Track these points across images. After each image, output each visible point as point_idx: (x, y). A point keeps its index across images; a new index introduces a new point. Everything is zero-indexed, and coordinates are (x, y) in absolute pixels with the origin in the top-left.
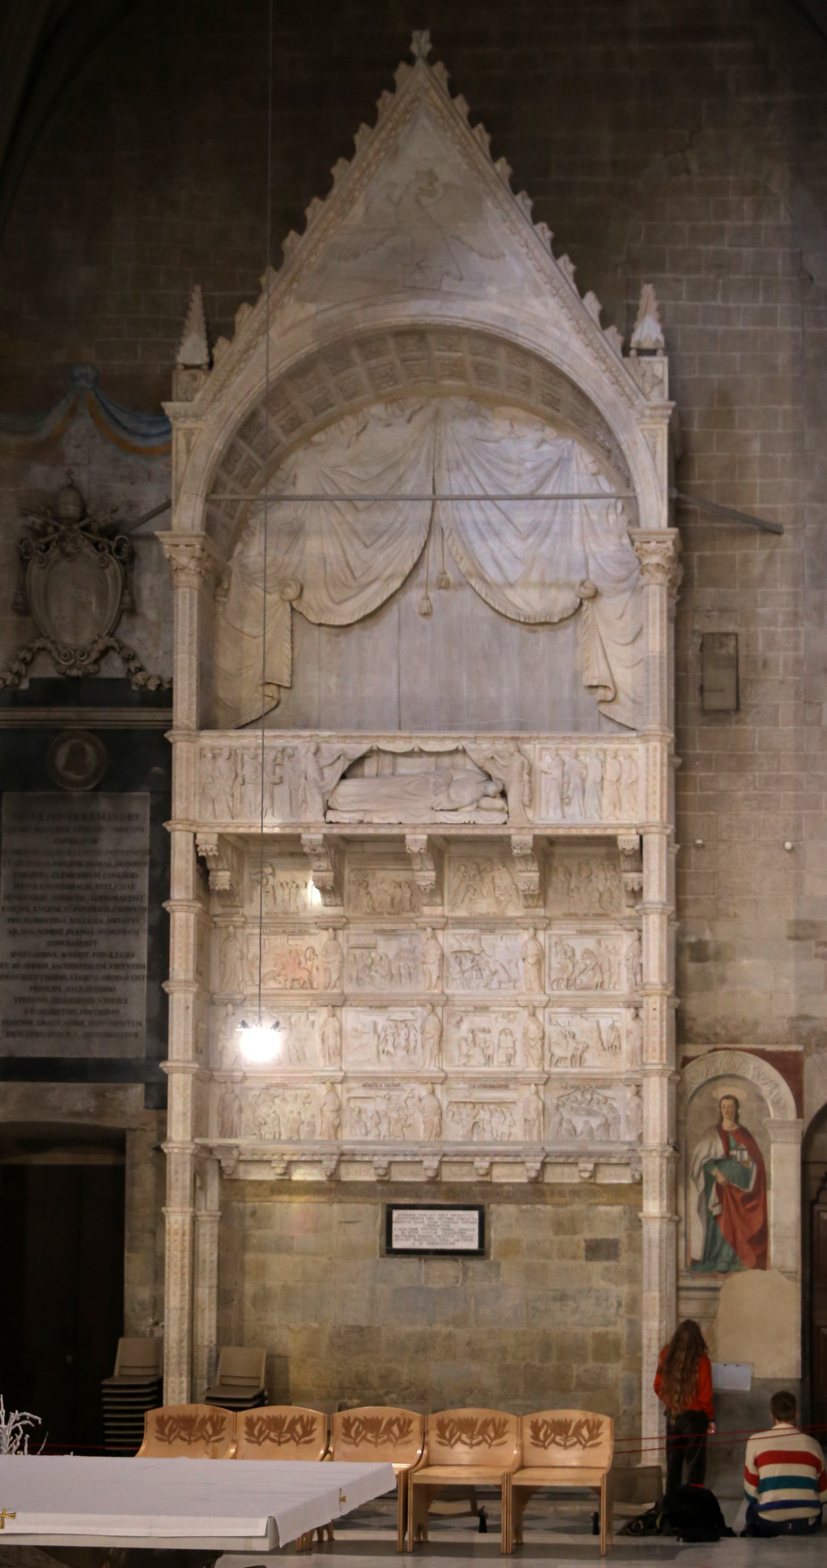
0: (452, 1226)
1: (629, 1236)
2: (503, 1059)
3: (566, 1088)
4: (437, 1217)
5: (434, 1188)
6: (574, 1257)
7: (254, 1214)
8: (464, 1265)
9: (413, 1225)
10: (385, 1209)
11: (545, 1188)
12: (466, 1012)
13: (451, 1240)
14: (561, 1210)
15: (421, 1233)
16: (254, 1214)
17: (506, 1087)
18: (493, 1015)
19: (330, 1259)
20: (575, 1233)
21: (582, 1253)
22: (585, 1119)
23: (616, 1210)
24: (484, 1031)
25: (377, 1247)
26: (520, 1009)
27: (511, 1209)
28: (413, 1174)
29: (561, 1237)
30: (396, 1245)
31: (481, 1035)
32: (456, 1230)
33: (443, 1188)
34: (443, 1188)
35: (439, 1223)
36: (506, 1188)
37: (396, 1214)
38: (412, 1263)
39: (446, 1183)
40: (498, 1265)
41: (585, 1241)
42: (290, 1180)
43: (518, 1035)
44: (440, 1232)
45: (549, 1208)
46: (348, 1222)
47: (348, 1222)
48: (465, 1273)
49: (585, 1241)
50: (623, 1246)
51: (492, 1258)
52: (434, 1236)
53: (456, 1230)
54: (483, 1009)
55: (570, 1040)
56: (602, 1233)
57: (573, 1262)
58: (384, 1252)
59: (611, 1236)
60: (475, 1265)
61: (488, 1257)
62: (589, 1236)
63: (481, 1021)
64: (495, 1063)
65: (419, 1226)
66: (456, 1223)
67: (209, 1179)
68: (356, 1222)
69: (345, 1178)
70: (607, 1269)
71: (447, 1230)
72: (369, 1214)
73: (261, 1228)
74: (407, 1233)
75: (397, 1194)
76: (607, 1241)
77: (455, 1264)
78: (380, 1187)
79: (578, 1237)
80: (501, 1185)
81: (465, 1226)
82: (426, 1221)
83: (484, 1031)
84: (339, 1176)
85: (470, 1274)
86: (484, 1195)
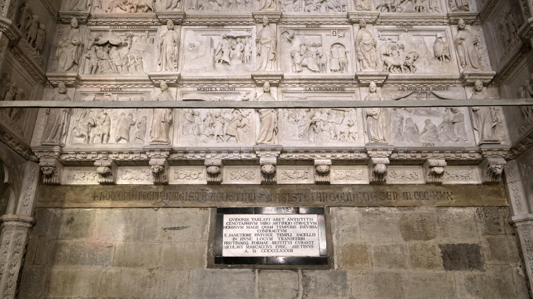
0: (289, 231)
1: (489, 240)
2: (336, 67)
3: (403, 90)
4: (272, 222)
5: (268, 191)
6: (431, 266)
7: (70, 221)
8: (304, 276)
9: (245, 231)
10: (215, 213)
11: (388, 190)
12: (298, 30)
13: (289, 246)
14: (408, 212)
15: (254, 239)
16: (70, 221)
17: (342, 90)
18: (323, 34)
19: (151, 270)
20: (428, 238)
21: (439, 260)
22: (426, 118)
23: (469, 212)
24: (314, 46)
25: (205, 256)
26: (350, 26)
27: (354, 211)
28: (245, 177)
29: (413, 242)
30: (226, 253)
31: (313, 49)
32: (294, 235)
33: (278, 190)
34: (278, 190)
35: (275, 227)
36: (346, 190)
37: (227, 218)
38: (243, 275)
39: (281, 185)
40: (344, 274)
41: (440, 246)
42: (113, 184)
43: (350, 46)
44: (275, 238)
45: (394, 210)
46: (174, 229)
47: (174, 229)
48: (306, 286)
49: (440, 246)
50: (485, 253)
51: (336, 267)
52: (270, 242)
53: (294, 235)
54: (313, 26)
55: (401, 51)
56: (457, 237)
57: (430, 271)
58: (213, 261)
59: (469, 241)
60: (318, 275)
61: (331, 267)
62: (445, 241)
63: (311, 38)
64: (328, 71)
65: (253, 231)
66: (294, 227)
67: (25, 182)
68: (183, 228)
69: (173, 181)
70: (471, 279)
71: (284, 236)
72: (198, 218)
73: (76, 237)
74: (238, 240)
75: (228, 197)
76: (466, 245)
77: (294, 274)
78: (210, 191)
79: (431, 242)
80: (341, 187)
81: (303, 231)
82: (260, 226)
83: (314, 46)
84: (166, 177)
85: (312, 285)
86: (323, 198)
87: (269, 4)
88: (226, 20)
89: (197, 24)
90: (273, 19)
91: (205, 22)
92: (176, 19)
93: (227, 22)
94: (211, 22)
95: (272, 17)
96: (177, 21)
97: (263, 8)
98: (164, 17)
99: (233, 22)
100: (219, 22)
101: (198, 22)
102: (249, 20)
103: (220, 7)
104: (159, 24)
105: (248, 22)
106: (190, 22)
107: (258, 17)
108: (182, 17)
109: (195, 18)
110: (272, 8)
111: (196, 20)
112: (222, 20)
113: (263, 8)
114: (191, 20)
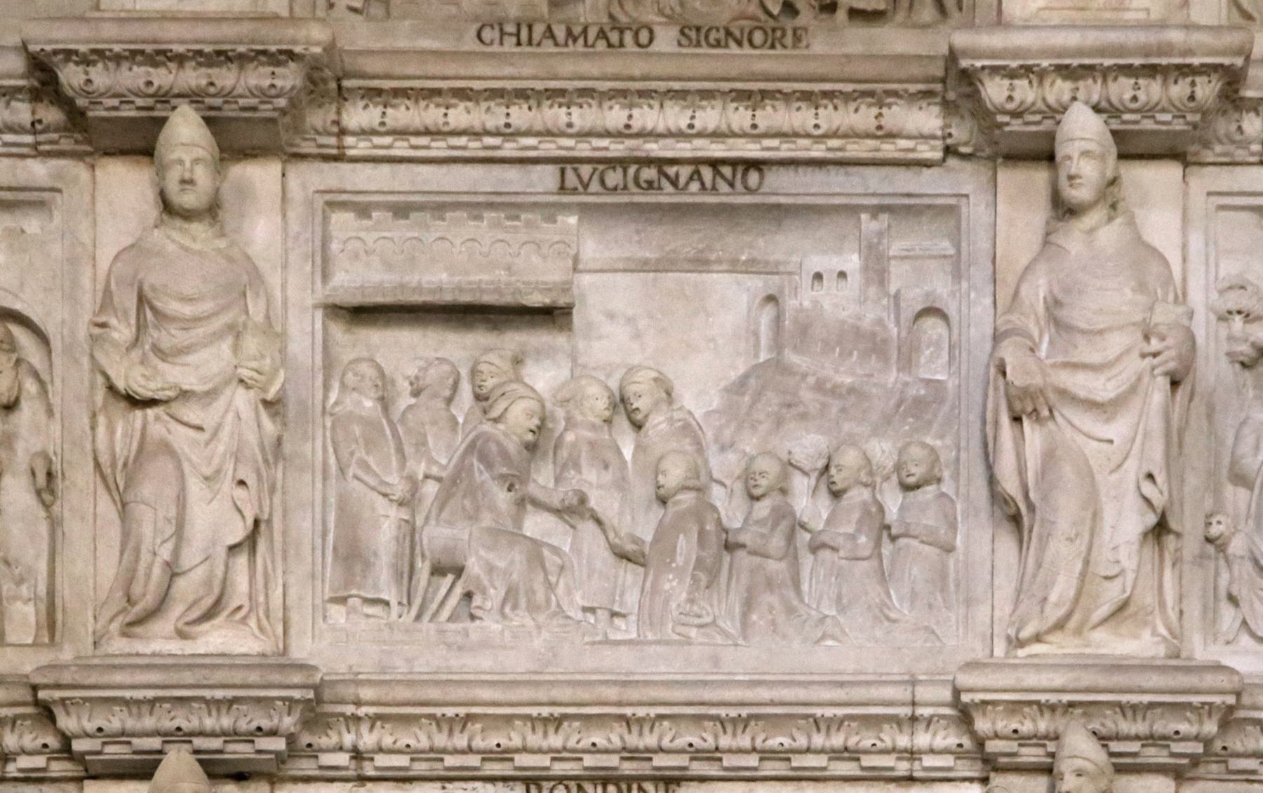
87: (1112, 594)
88: (704, 738)
89: (421, 768)
90: (1151, 739)
91: (503, 754)
92: (232, 735)
93: (713, 755)
94: (558, 755)
95: (1140, 728)
96: (241, 750)
97: (1059, 626)
98: (116, 721)
99: (767, 755)
100: (631, 754)
101: (437, 753)
102: (922, 739)
103: (629, 575)
104: (59, 768)
105: (912, 754)
106: (358, 755)
107: (1005, 724)
108: (288, 722)
109: (407, 720)
110: (1143, 619)
111: (419, 738)
112: (666, 735)
113: (1059, 626)
114: (368, 740)
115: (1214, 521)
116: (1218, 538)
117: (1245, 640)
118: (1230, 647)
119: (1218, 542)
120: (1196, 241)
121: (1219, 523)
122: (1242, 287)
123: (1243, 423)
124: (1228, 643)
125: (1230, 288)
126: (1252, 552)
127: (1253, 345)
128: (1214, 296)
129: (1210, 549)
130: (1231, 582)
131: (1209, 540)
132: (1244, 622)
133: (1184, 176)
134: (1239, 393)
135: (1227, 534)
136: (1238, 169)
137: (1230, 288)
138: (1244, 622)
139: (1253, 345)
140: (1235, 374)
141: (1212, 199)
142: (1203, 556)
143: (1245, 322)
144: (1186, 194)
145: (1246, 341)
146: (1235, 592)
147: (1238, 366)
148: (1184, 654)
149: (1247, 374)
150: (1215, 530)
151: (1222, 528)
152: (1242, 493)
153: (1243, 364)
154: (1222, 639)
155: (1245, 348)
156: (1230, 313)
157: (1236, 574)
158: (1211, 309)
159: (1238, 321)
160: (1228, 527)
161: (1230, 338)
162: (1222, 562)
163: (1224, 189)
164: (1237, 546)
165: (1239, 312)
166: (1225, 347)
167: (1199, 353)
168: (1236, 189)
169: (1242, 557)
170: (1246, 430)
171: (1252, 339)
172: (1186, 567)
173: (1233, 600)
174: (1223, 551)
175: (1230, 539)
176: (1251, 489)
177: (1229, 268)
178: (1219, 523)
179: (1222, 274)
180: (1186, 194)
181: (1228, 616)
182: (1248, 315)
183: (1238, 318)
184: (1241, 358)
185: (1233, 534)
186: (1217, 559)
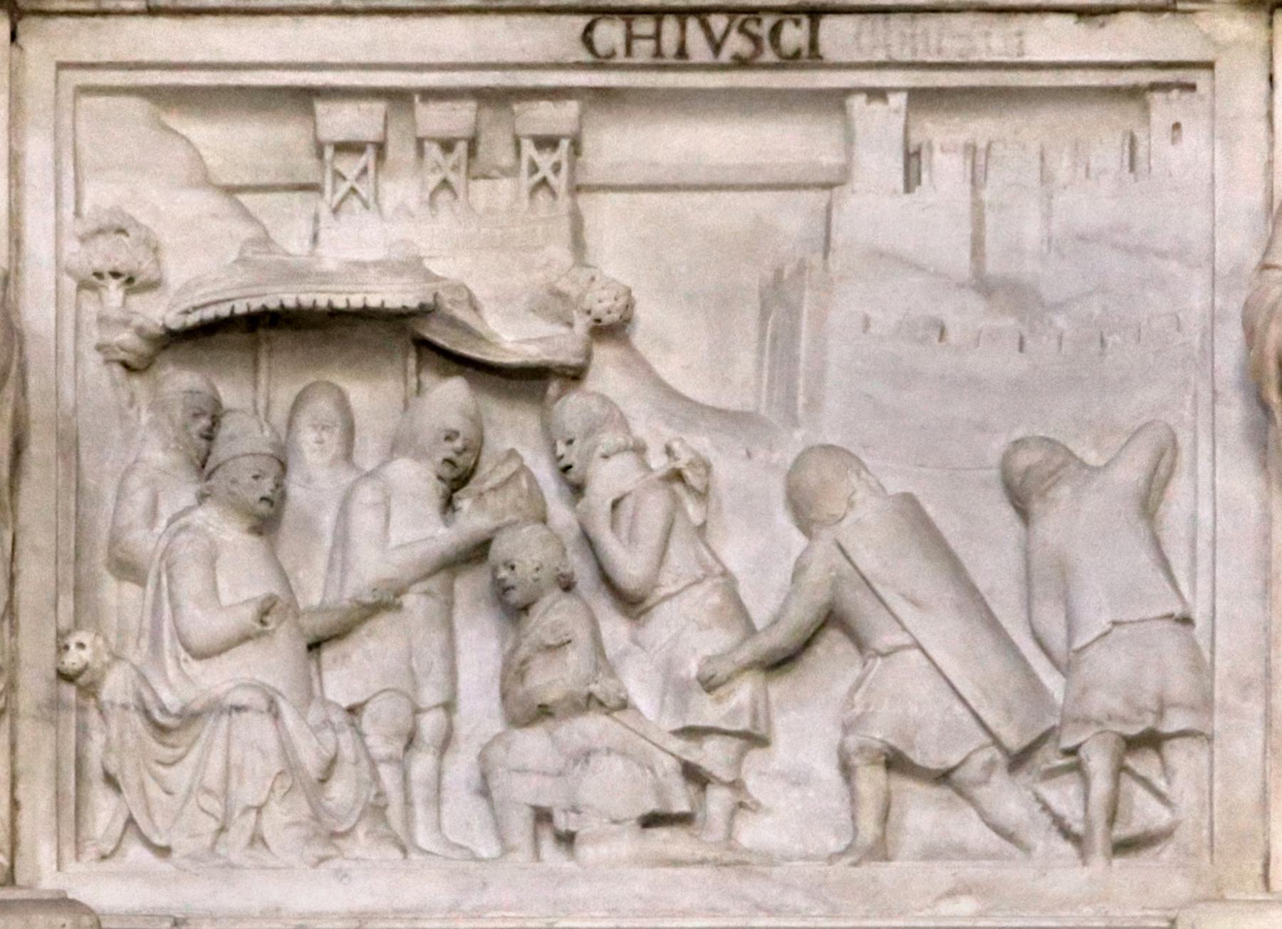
115: (72, 642)
116: (80, 673)
117: (135, 852)
118: (107, 865)
119: (81, 680)
120: (37, 149)
121: (81, 646)
122: (121, 231)
123: (130, 470)
124: (104, 857)
125: (100, 231)
126: (140, 698)
127: (140, 331)
128: (72, 247)
129: (70, 692)
130: (108, 747)
131: (64, 677)
132: (130, 821)
133: (13, 37)
134: (123, 417)
135: (98, 666)
136: (111, 20)
137: (100, 231)
138: (130, 821)
139: (140, 331)
140: (115, 384)
141: (66, 74)
142: (56, 704)
143: (127, 293)
144: (14, 73)
145: (126, 323)
146: (113, 770)
147: (118, 369)
148: (21, 878)
149: (136, 382)
150: (73, 659)
151: (86, 655)
152: (130, 590)
153: (126, 365)
154: (90, 852)
155: (126, 337)
156: (99, 275)
157: (114, 733)
158: (61, 267)
159: (114, 292)
160: (96, 654)
161: (102, 320)
162: (93, 717)
163: (87, 58)
164: (116, 685)
165: (116, 275)
166: (94, 336)
167: (32, 351)
168: (106, 58)
169: (125, 707)
170: (135, 482)
171: (138, 321)
172: (26, 728)
173: (111, 781)
174: (95, 695)
175: (103, 675)
176: (141, 582)
177: (101, 195)
178: (81, 646)
179: (86, 208)
180: (14, 73)
181: (105, 811)
182: (130, 280)
183: (113, 284)
184: (122, 355)
185: (108, 666)
186: (81, 709)
